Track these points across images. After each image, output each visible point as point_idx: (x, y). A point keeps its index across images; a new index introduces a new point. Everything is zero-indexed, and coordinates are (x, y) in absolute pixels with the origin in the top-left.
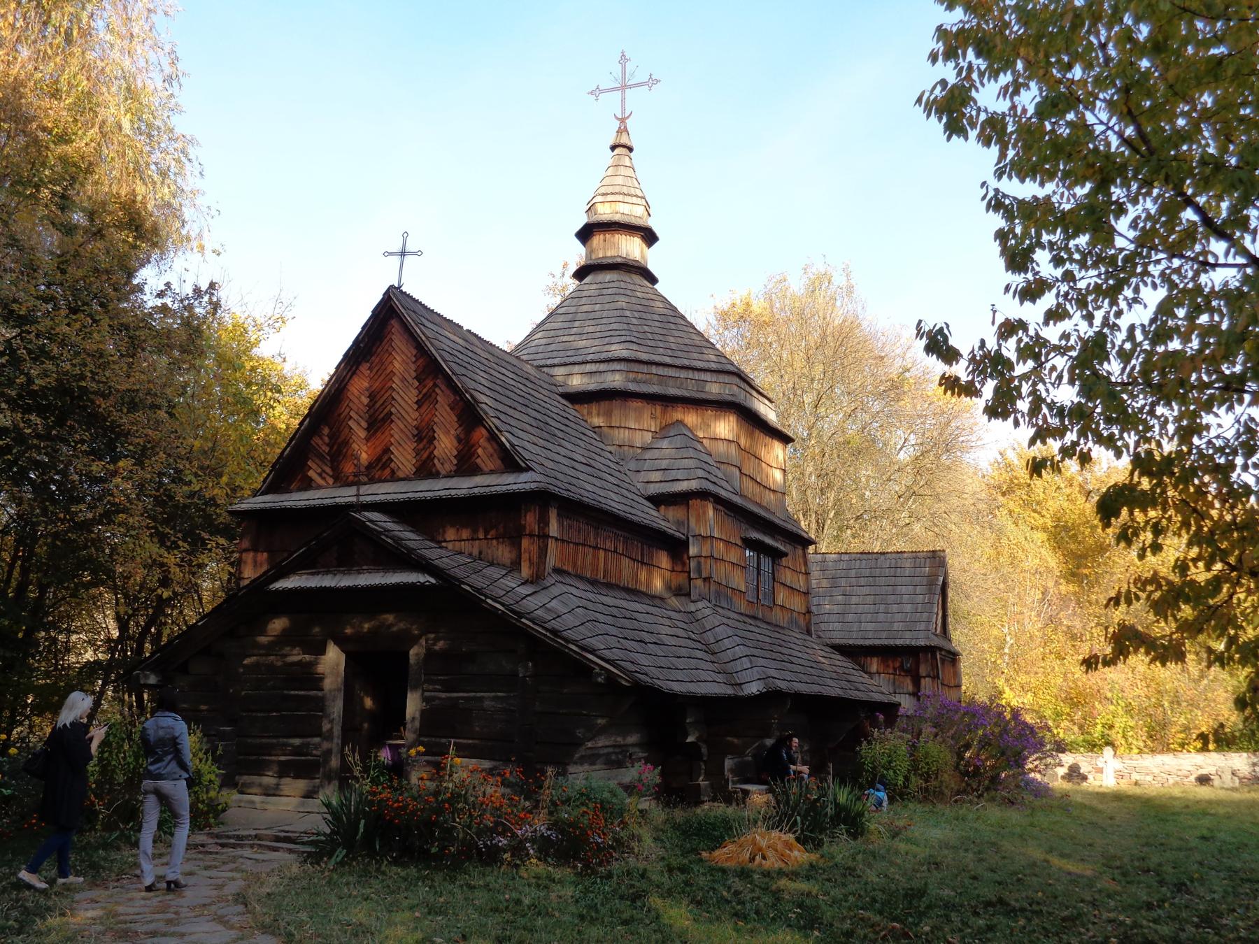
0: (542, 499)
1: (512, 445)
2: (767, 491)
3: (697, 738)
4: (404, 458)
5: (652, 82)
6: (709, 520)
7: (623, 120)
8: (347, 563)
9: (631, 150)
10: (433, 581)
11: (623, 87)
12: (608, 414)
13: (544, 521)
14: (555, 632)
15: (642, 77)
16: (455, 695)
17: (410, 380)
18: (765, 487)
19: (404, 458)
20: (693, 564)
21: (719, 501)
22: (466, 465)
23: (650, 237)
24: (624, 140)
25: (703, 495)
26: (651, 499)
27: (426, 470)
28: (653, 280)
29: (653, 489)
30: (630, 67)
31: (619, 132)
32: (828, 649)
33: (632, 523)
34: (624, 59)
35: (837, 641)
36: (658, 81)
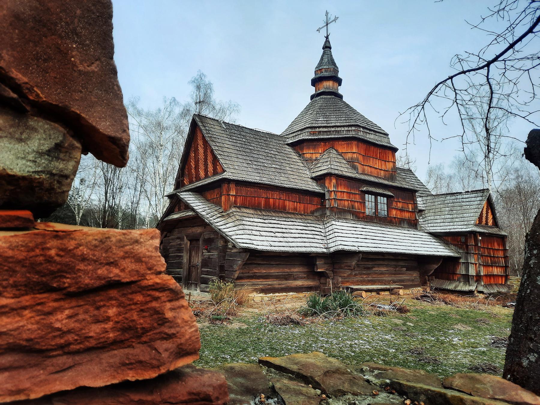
0: (228, 181)
1: (222, 163)
2: (382, 172)
3: (327, 269)
4: (202, 174)
5: (336, 19)
6: (331, 185)
7: (327, 37)
8: (180, 210)
9: (330, 48)
11: (327, 25)
12: (302, 149)
13: (229, 190)
14: (219, 229)
15: (333, 18)
16: (210, 253)
17: (202, 145)
18: (381, 170)
19: (202, 174)
20: (327, 201)
21: (339, 177)
22: (215, 173)
23: (339, 81)
24: (327, 45)
25: (329, 175)
26: (312, 178)
27: (207, 176)
28: (341, 97)
29: (314, 175)
30: (329, 16)
31: (326, 42)
32: (427, 234)
33: (285, 188)
34: (327, 13)
35: (430, 231)
36: (338, 18)
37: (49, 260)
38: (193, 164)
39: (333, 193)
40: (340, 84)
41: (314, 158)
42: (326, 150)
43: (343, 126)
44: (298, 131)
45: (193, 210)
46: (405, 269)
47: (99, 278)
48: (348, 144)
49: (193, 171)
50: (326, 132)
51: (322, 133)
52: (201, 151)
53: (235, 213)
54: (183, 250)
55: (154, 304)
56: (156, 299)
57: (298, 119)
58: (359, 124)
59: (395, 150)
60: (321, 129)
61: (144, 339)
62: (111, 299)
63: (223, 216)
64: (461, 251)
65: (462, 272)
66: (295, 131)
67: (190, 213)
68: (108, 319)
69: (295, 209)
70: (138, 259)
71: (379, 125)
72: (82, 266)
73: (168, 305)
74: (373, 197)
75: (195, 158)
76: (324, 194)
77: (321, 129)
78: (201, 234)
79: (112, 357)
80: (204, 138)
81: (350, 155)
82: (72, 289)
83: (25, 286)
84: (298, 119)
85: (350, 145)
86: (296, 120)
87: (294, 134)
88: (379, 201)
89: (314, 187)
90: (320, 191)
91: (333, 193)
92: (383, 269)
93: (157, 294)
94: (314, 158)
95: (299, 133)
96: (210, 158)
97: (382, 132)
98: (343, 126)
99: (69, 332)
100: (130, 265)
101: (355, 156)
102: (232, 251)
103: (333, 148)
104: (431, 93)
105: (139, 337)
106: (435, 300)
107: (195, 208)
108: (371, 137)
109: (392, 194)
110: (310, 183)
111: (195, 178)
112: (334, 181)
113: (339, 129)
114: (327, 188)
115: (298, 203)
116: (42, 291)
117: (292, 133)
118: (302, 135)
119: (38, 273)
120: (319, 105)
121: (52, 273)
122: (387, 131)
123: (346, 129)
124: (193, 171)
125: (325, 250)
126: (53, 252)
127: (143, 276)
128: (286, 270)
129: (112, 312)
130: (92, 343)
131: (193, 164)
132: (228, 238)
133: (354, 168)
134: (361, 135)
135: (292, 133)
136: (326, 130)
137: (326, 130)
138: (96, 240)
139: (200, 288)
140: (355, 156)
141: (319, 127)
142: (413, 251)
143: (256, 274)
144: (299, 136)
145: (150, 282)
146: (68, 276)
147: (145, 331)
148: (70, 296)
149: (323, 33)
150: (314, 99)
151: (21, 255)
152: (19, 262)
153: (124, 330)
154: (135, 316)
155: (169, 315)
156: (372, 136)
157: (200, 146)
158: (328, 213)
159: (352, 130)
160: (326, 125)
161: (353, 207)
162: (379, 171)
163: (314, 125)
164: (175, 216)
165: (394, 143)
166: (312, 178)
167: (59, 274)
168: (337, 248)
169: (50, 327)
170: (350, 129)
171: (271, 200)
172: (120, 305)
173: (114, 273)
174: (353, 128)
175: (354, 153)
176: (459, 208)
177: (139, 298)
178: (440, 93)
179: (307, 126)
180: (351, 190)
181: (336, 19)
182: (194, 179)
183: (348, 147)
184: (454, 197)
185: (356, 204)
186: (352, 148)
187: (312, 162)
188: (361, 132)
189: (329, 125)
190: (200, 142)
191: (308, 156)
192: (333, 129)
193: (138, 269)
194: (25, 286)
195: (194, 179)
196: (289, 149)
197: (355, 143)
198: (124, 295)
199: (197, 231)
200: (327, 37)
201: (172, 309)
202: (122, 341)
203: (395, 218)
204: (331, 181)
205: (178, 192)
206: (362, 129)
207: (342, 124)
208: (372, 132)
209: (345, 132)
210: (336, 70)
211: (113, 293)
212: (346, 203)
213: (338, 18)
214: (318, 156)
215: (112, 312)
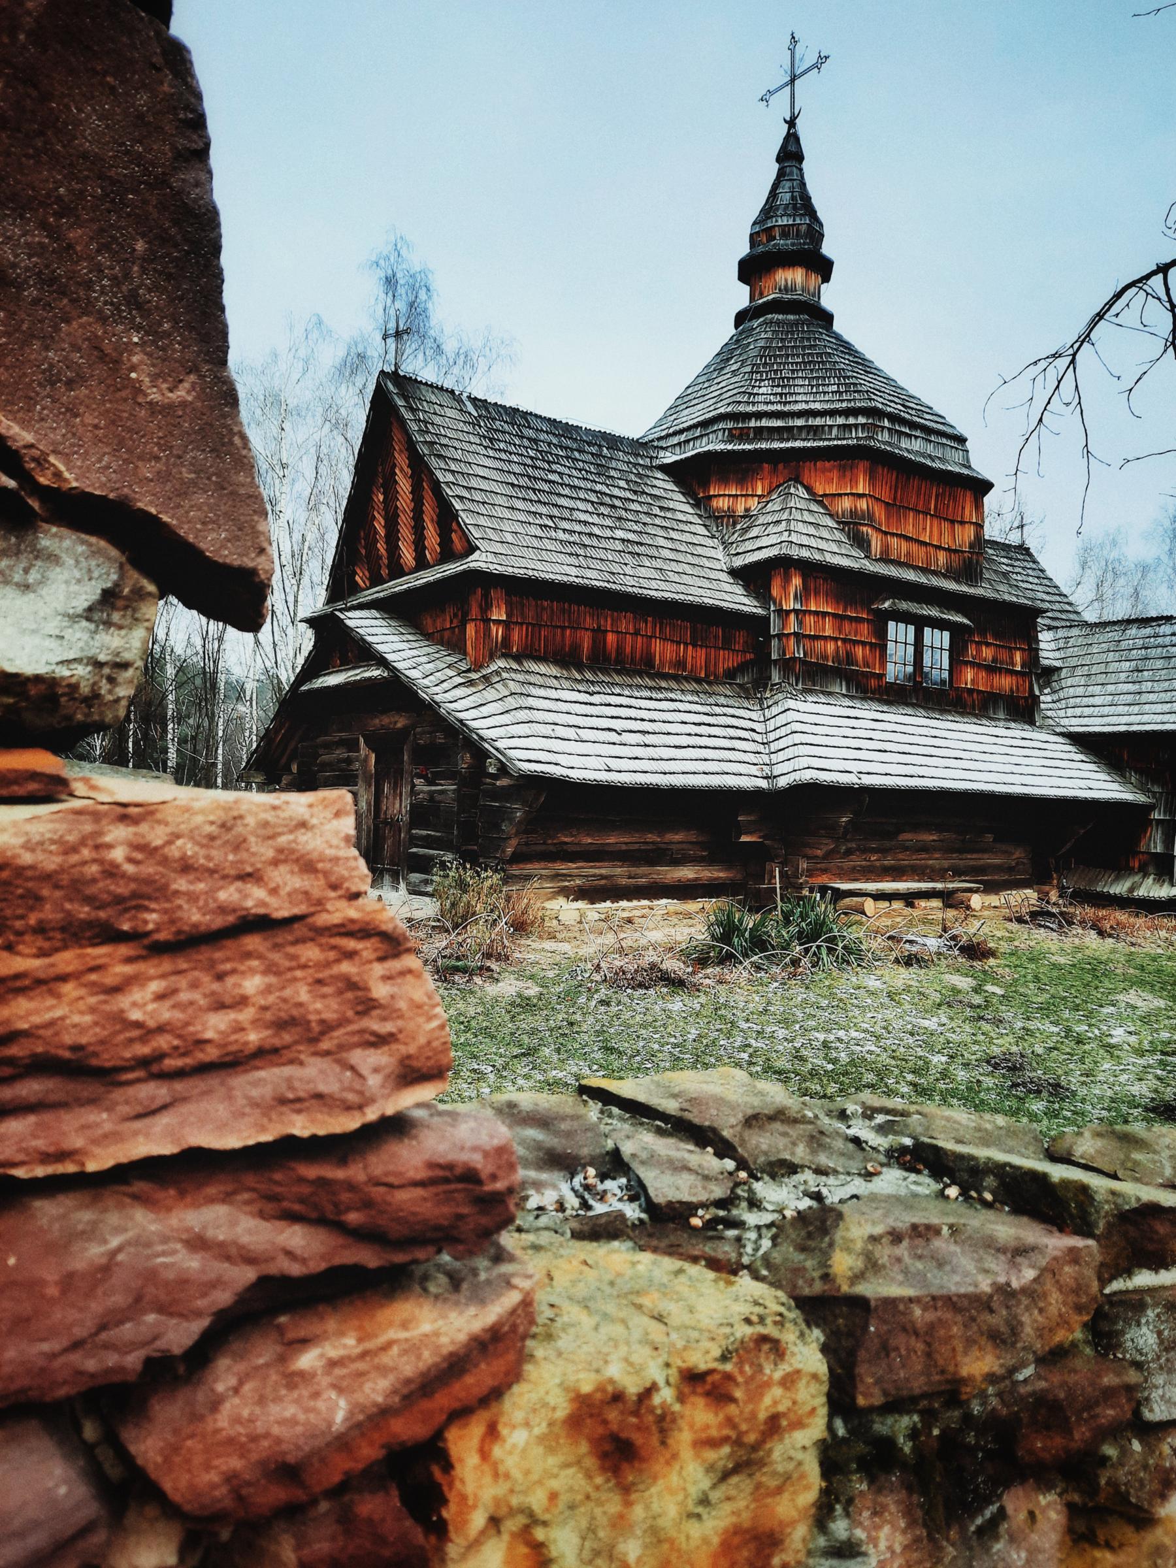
1: (466, 524)
5: (823, 59)
7: (791, 123)
10: (386, 674)
11: (792, 81)
12: (706, 485)
14: (461, 721)
15: (811, 59)
16: (433, 788)
17: (405, 468)
18: (938, 547)
20: (774, 643)
22: (447, 554)
23: (823, 268)
24: (792, 148)
25: (783, 564)
26: (734, 573)
28: (826, 318)
29: (738, 562)
32: (1060, 739)
35: (1072, 729)
36: (826, 58)
37: (112, 871)
38: (379, 526)
39: (792, 616)
40: (826, 278)
41: (740, 510)
42: (778, 487)
43: (832, 413)
44: (695, 426)
45: (382, 662)
46: (989, 837)
47: (222, 910)
48: (842, 470)
49: (381, 547)
50: (778, 429)
51: (765, 435)
52: (404, 485)
53: (505, 675)
54: (356, 776)
55: (346, 967)
56: (350, 955)
57: (696, 388)
58: (880, 406)
59: (985, 486)
60: (765, 423)
61: (325, 1045)
62: (248, 955)
63: (471, 683)
64: (1156, 789)
65: (1155, 847)
66: (685, 425)
67: (375, 673)
68: (242, 1001)
69: (680, 664)
70: (308, 866)
71: (937, 409)
72: (181, 884)
73: (379, 969)
74: (911, 629)
75: (386, 509)
76: (766, 620)
77: (765, 423)
78: (405, 731)
79: (256, 1084)
80: (411, 446)
81: (846, 504)
82: (162, 936)
83: (63, 929)
84: (696, 388)
85: (848, 474)
86: (689, 391)
87: (683, 438)
88: (927, 640)
89: (736, 598)
90: (755, 610)
91: (792, 616)
92: (930, 837)
93: (351, 944)
94: (740, 510)
95: (698, 432)
96: (429, 509)
97: (949, 430)
98: (832, 413)
99: (161, 1029)
100: (288, 879)
101: (863, 504)
102: (498, 783)
103: (798, 480)
104: (1100, 316)
105: (314, 1040)
106: (1070, 923)
107: (390, 657)
108: (913, 447)
109: (966, 621)
110: (727, 587)
111: (388, 567)
112: (796, 581)
113: (818, 421)
114: (775, 604)
115: (690, 648)
116: (98, 940)
117: (675, 434)
118: (705, 440)
119: (89, 900)
120: (762, 343)
121: (119, 900)
122: (962, 429)
123: (840, 421)
124: (381, 547)
125: (763, 784)
126: (118, 854)
127: (320, 902)
128: (651, 837)
129: (252, 984)
130: (211, 1054)
131: (379, 526)
132: (487, 746)
133: (860, 542)
134: (882, 439)
135: (675, 434)
136: (779, 423)
137: (779, 423)
138: (212, 823)
139: (408, 884)
140: (863, 504)
141: (759, 415)
142: (1016, 786)
143: (565, 847)
144: (698, 443)
145: (335, 918)
146: (153, 906)
147: (327, 1027)
148: (159, 949)
149: (781, 106)
150: (747, 325)
151: (51, 863)
152: (47, 877)
153: (281, 1025)
154: (303, 994)
155: (380, 991)
156: (917, 445)
157: (402, 470)
158: (776, 677)
159: (856, 426)
160: (779, 407)
161: (850, 659)
162: (932, 550)
163: (742, 408)
164: (333, 680)
165: (982, 464)
166: (734, 573)
167: (134, 901)
168: (798, 778)
169: (119, 1018)
170: (852, 421)
171: (611, 637)
172: (270, 969)
173: (255, 898)
174: (862, 420)
175: (860, 496)
176: (1159, 664)
177: (311, 953)
178: (1130, 317)
179: (722, 410)
180: (845, 610)
181: (823, 59)
182: (384, 572)
183: (842, 477)
184: (1148, 631)
185: (859, 652)
186: (854, 482)
187: (734, 524)
188: (886, 432)
189: (787, 408)
190: (401, 460)
191: (722, 504)
192: (800, 422)
193: (308, 888)
194: (63, 929)
195: (384, 572)
196: (663, 484)
197: (862, 465)
198: (276, 947)
199: (396, 723)
200: (791, 123)
201: (387, 978)
202: (275, 1051)
203: (970, 691)
204: (787, 580)
205: (340, 610)
206: (886, 423)
207: (827, 406)
208: (918, 433)
209: (835, 431)
210: (815, 234)
211: (253, 942)
212: (831, 647)
213: (826, 58)
214: (753, 503)
215: (252, 984)
